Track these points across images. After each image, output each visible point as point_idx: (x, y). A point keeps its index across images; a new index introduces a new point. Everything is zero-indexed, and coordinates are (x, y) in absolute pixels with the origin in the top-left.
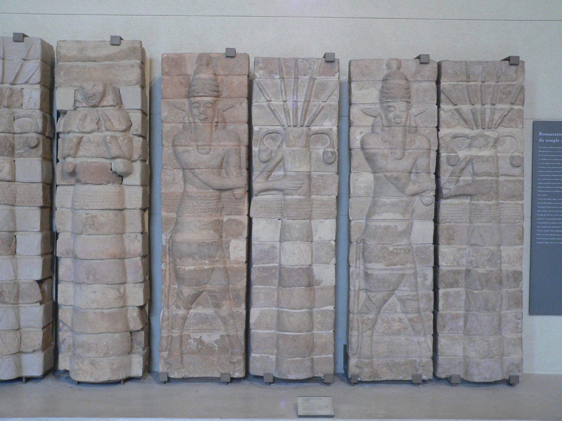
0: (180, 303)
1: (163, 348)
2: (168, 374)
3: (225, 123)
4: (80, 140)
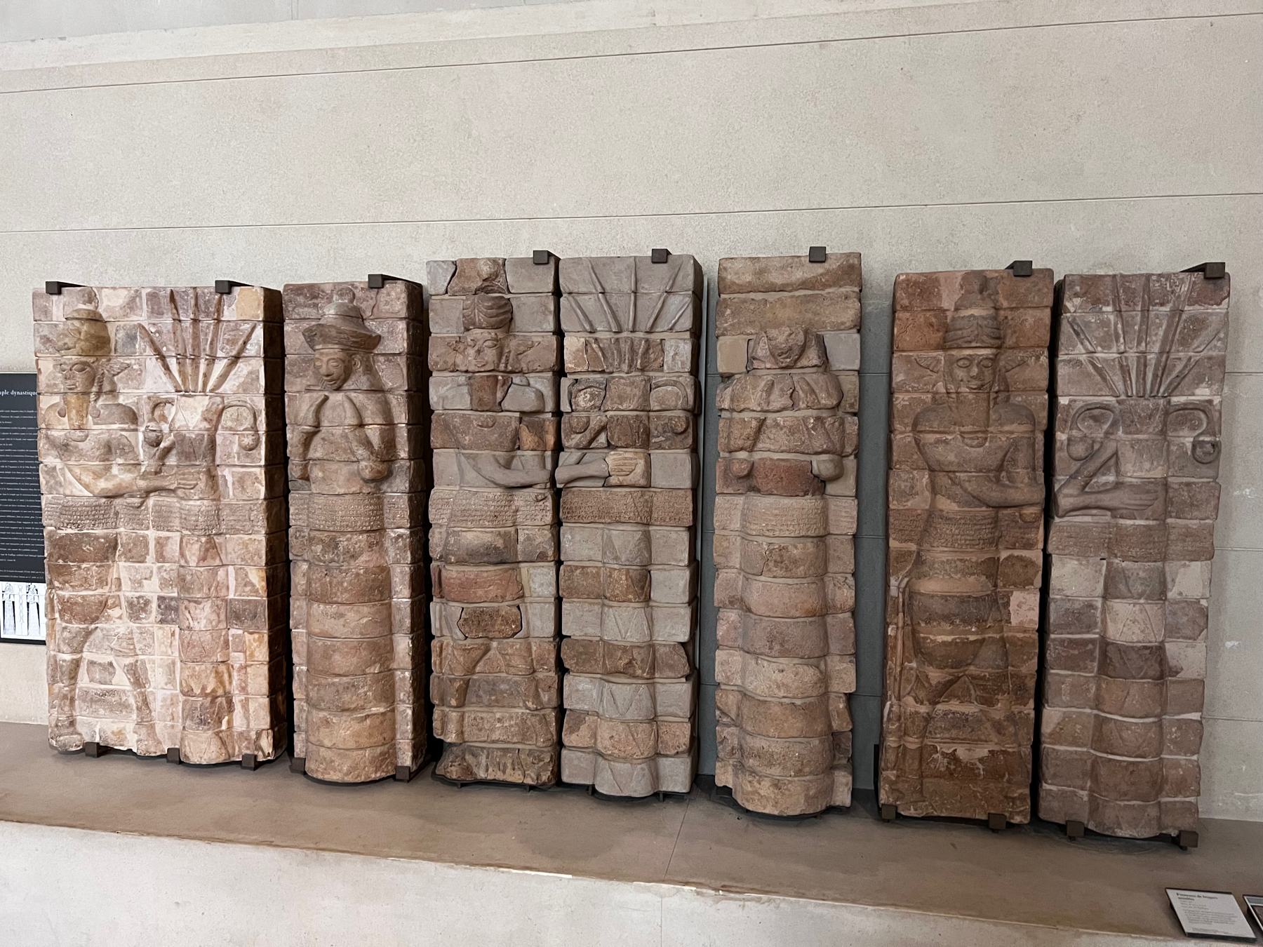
0: (922, 694)
1: (889, 765)
2: (896, 807)
3: (1008, 391)
4: (762, 423)
